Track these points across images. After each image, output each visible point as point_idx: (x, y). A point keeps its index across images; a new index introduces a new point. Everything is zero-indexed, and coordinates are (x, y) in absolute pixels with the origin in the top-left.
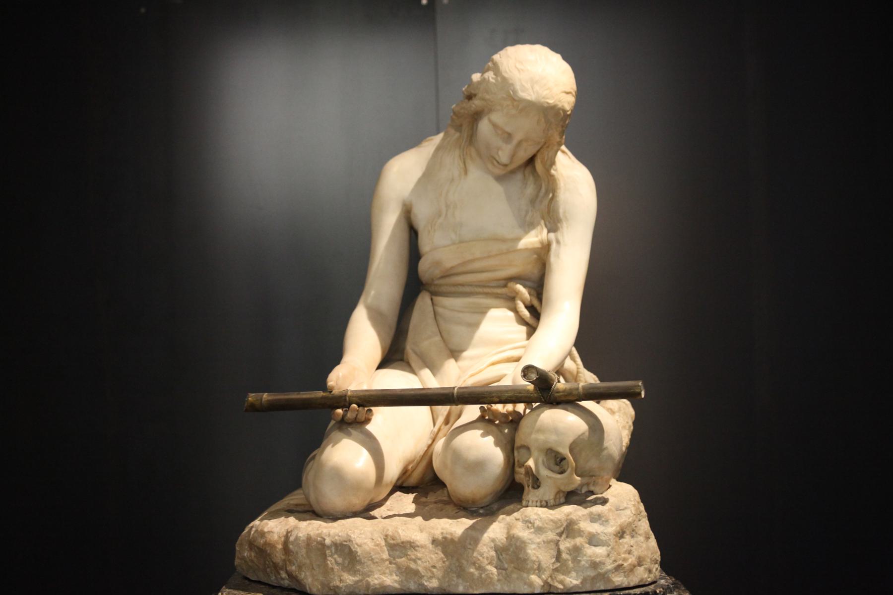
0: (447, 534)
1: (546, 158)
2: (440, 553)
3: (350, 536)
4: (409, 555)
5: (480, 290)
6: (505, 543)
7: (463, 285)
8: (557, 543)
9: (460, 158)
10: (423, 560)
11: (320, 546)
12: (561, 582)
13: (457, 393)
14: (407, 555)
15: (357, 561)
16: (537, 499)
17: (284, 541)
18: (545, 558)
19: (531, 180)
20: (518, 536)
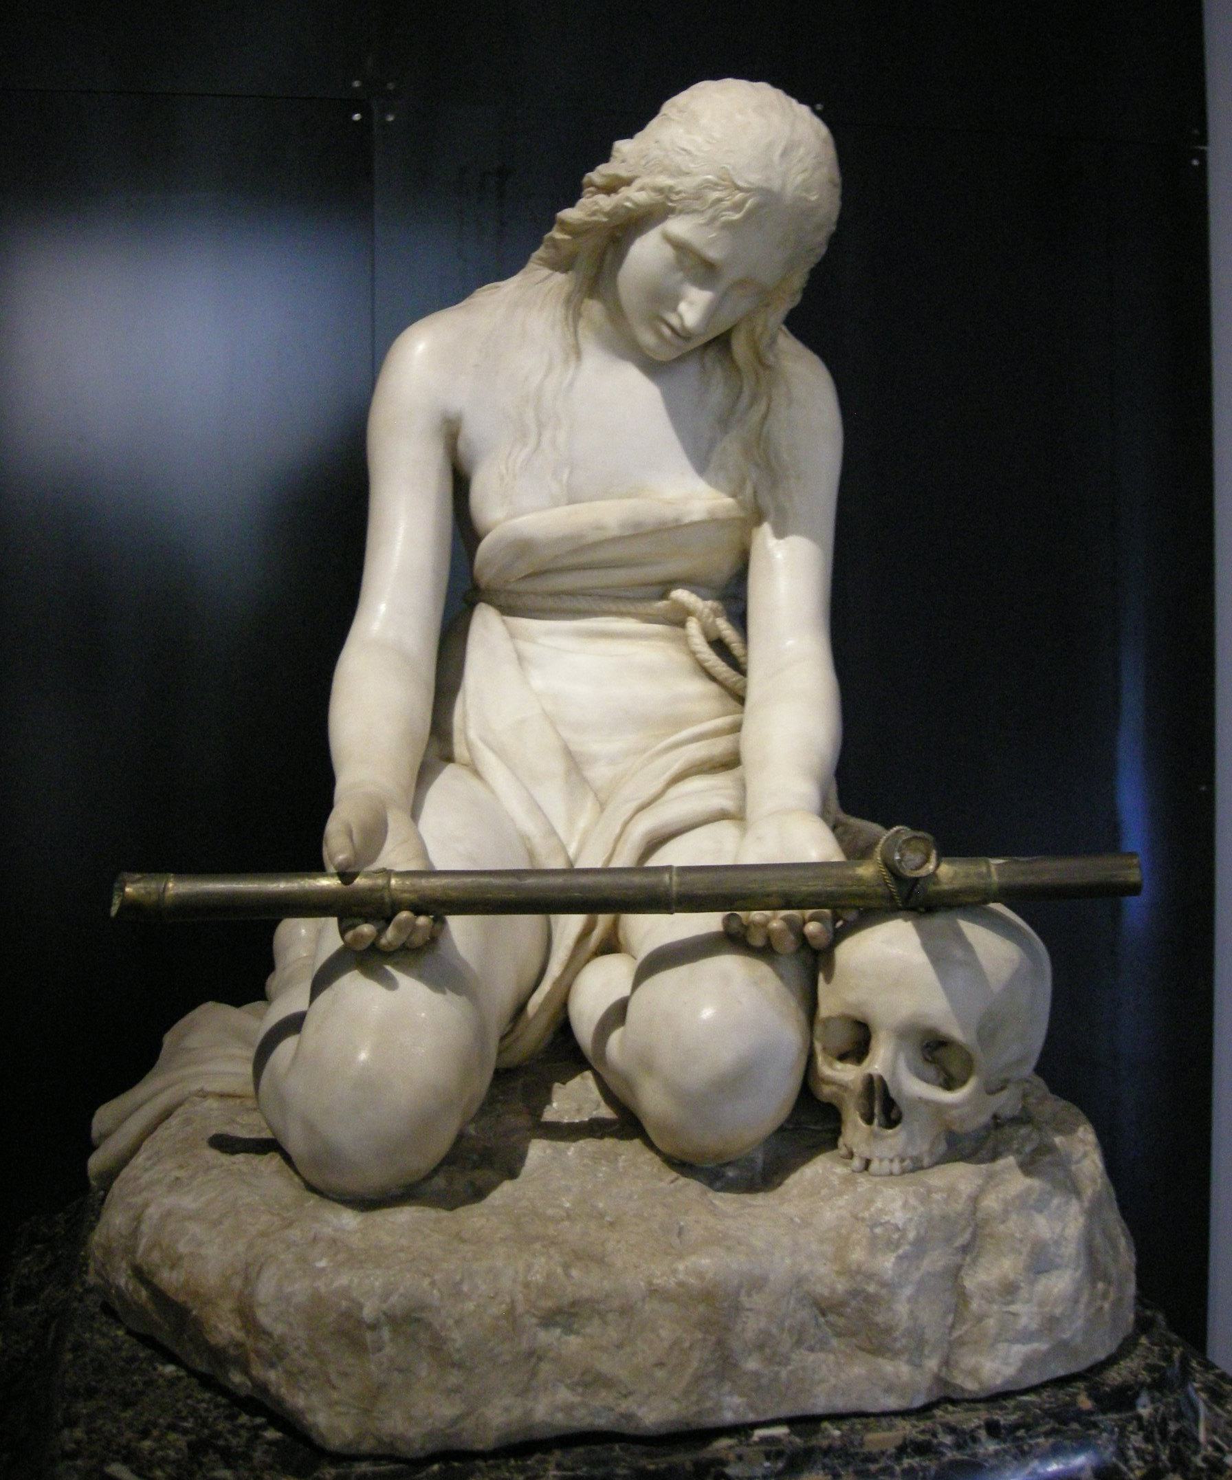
1: (759, 329)
5: (613, 607)
7: (571, 593)
8: (955, 1274)
9: (567, 324)
12: (973, 1373)
13: (680, 884)
16: (891, 1155)
18: (931, 1318)
19: (718, 375)
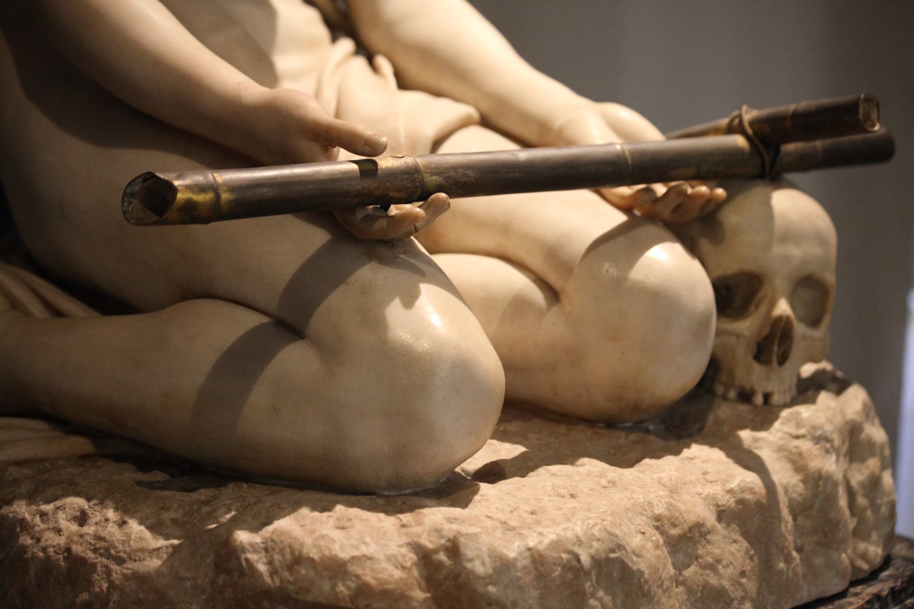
0: (742, 492)
2: (740, 538)
3: (616, 536)
4: (701, 557)
6: (804, 492)
10: (724, 563)
11: (570, 576)
14: (697, 557)
15: (644, 595)
17: (421, 576)
20: (827, 472)
